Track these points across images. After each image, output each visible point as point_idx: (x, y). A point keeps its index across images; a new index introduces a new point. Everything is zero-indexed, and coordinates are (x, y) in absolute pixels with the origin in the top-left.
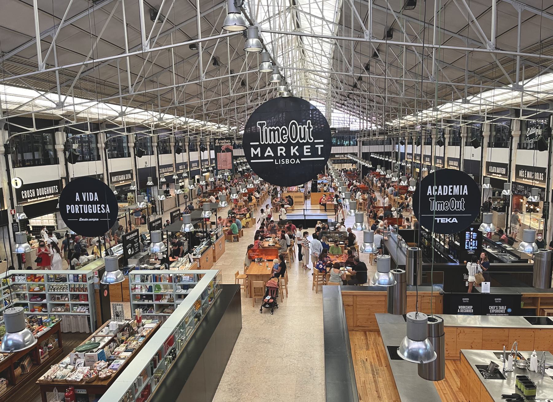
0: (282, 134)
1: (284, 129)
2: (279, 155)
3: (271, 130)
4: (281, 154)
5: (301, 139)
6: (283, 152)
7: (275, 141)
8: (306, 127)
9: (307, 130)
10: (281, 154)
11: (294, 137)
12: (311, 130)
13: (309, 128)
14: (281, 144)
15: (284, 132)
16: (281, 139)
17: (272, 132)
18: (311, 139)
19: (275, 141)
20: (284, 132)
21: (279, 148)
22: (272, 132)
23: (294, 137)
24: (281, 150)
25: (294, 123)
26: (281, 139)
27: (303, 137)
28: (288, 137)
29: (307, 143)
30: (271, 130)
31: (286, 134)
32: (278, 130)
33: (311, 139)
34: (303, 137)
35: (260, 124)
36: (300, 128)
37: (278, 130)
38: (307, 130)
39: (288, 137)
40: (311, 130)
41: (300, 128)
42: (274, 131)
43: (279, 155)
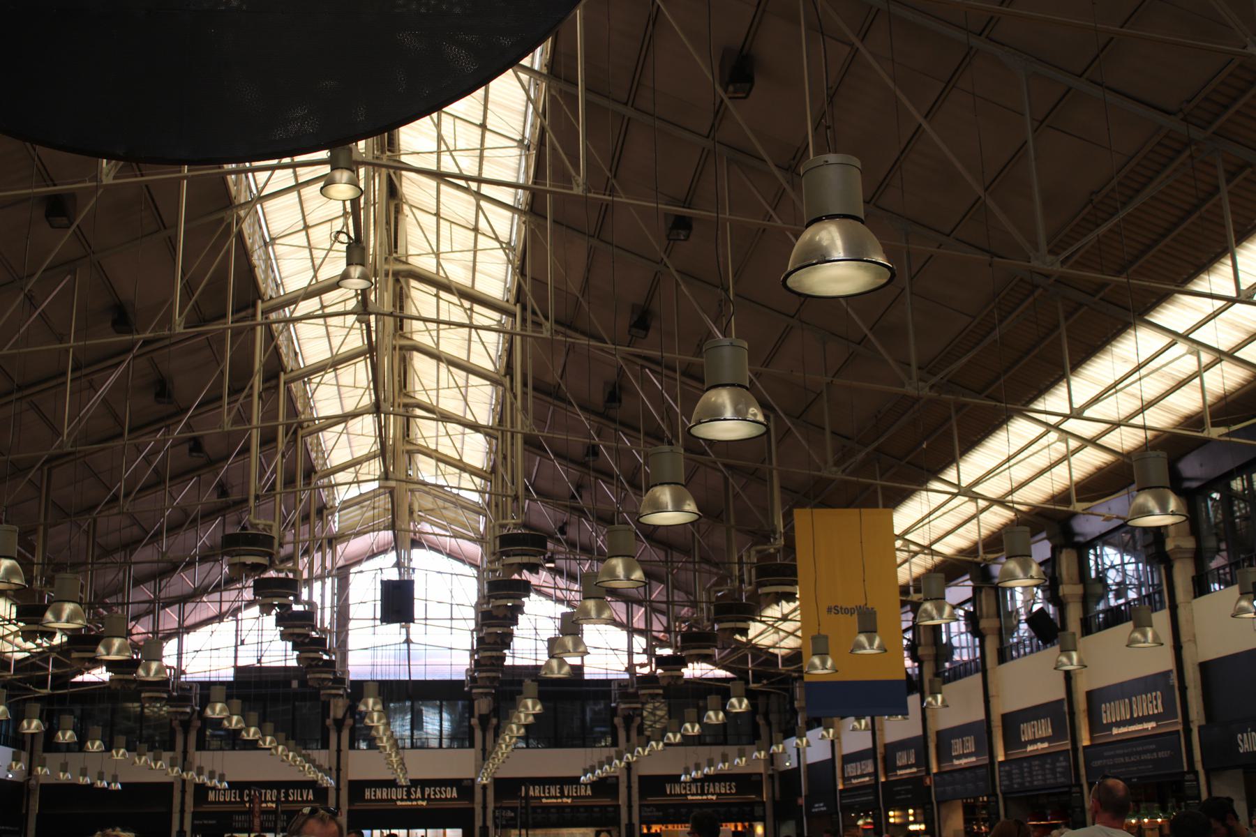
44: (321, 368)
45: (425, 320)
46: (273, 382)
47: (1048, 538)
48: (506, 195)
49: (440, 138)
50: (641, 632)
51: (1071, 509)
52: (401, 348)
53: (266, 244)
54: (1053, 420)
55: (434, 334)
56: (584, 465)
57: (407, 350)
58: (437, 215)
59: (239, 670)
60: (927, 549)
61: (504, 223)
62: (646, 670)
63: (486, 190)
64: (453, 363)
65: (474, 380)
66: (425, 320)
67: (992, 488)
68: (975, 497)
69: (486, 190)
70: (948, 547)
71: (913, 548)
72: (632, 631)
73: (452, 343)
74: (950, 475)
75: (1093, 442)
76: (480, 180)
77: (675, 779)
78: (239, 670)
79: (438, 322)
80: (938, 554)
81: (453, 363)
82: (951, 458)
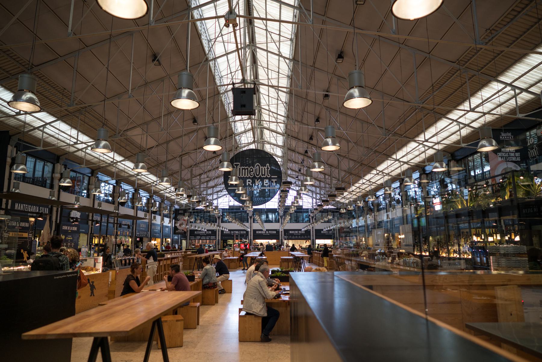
0: (250, 172)
1: (251, 168)
2: (247, 185)
3: (243, 169)
4: (249, 184)
5: (262, 175)
6: (250, 183)
7: (245, 175)
8: (266, 168)
9: (266, 169)
10: (249, 184)
11: (258, 174)
12: (269, 169)
13: (268, 168)
14: (249, 178)
15: (251, 170)
16: (249, 175)
17: (244, 170)
18: (269, 176)
19: (245, 175)
20: (251, 170)
21: (247, 180)
22: (244, 170)
23: (258, 174)
24: (249, 181)
25: (258, 165)
26: (249, 175)
27: (263, 174)
28: (254, 173)
29: (266, 178)
30: (243, 169)
31: (252, 171)
32: (247, 169)
33: (269, 176)
34: (263, 174)
35: (235, 165)
36: (262, 168)
37: (247, 169)
38: (266, 169)
39: (254, 173)
40: (269, 169)
41: (262, 168)
42: (245, 169)
43: (247, 185)
44: (242, 133)
45: (266, 121)
46: (231, 137)
47: (419, 172)
48: (285, 90)
49: (268, 78)
50: (314, 198)
51: (425, 164)
52: (261, 128)
53: (229, 104)
54: (421, 142)
55: (268, 124)
56: (304, 155)
57: (262, 129)
58: (268, 96)
59: (230, 206)
60: (388, 174)
61: (284, 97)
62: (320, 203)
63: (280, 88)
64: (272, 131)
65: (278, 135)
66: (266, 121)
67: (405, 159)
68: (400, 162)
69: (280, 88)
70: (394, 174)
71: (384, 174)
72: (313, 198)
73: (273, 126)
74: (394, 156)
75: (432, 147)
76: (278, 87)
77: (323, 230)
78: (230, 206)
79: (269, 121)
80: (391, 176)
81: (272, 131)
82: (395, 152)
